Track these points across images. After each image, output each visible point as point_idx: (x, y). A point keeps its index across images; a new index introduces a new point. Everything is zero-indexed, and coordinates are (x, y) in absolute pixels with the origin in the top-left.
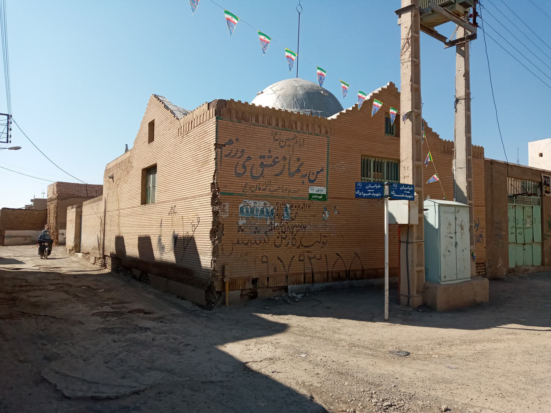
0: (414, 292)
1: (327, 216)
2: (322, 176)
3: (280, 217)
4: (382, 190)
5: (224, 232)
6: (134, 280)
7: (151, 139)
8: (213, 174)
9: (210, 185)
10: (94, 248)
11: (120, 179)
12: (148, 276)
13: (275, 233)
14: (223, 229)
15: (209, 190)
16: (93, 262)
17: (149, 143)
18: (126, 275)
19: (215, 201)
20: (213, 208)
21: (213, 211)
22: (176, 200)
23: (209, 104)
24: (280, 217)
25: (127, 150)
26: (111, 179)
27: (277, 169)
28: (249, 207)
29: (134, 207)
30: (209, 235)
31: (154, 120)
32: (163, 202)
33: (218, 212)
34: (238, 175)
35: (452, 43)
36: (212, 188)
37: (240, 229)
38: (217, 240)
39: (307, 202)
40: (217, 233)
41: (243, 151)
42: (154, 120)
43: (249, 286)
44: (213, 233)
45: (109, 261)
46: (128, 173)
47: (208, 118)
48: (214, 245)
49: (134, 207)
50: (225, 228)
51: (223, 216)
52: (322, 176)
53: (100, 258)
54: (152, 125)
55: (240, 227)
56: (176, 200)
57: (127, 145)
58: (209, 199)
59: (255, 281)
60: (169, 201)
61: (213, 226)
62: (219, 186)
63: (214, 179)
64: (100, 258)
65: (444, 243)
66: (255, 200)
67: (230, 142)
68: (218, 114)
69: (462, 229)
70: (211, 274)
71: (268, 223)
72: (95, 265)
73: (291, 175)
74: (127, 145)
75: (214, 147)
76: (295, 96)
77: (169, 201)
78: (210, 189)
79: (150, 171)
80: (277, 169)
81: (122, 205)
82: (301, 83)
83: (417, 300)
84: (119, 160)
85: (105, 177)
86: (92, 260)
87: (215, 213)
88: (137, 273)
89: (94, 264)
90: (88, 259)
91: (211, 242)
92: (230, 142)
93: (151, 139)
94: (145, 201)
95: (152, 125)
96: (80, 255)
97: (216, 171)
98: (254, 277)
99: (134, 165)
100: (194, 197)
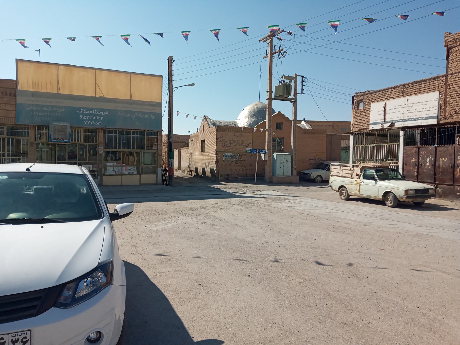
0: (267, 178)
2: (251, 145)
3: (236, 158)
4: (257, 151)
7: (204, 131)
10: (187, 168)
13: (234, 162)
19: (216, 154)
24: (236, 158)
27: (235, 144)
34: (223, 146)
35: (292, 102)
37: (223, 161)
39: (245, 153)
43: (226, 176)
44: (216, 162)
52: (251, 145)
54: (204, 125)
59: (228, 175)
65: (278, 165)
67: (221, 138)
68: (217, 130)
69: (287, 161)
73: (240, 145)
76: (254, 112)
79: (203, 141)
80: (235, 144)
82: (258, 106)
83: (268, 180)
86: (186, 172)
87: (216, 157)
90: (184, 172)
92: (221, 138)
93: (204, 131)
94: (202, 151)
95: (204, 125)
96: (181, 171)
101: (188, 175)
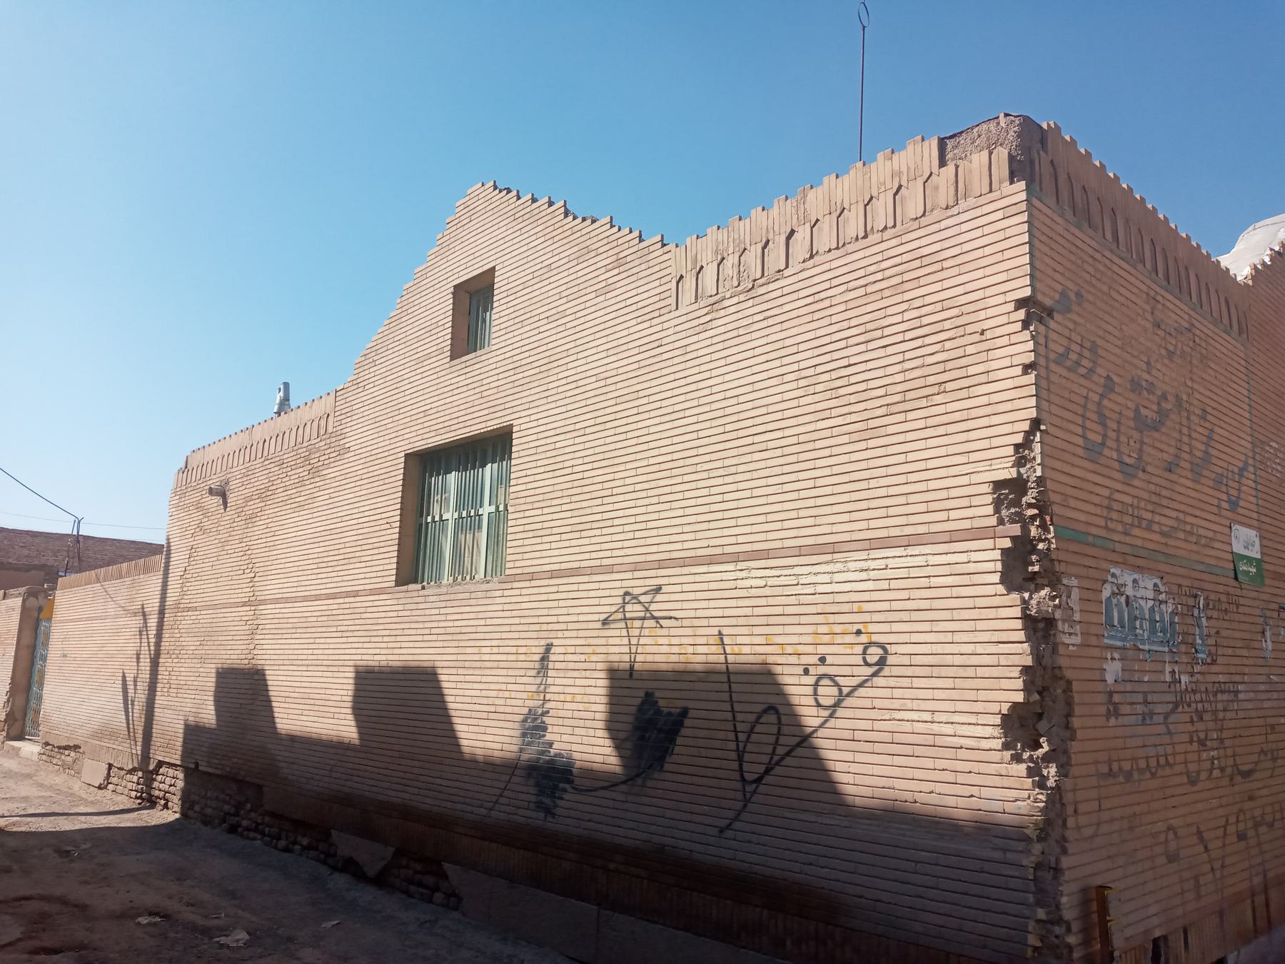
1: (1269, 643)
5: (1076, 722)
6: (340, 881)
8: (1019, 439)
9: (987, 488)
10: (105, 733)
11: (264, 495)
12: (444, 876)
14: (1069, 703)
15: (984, 511)
16: (99, 780)
17: (453, 358)
18: (286, 850)
19: (1019, 568)
20: (1025, 604)
21: (1026, 617)
22: (660, 564)
23: (942, 144)
25: (284, 405)
26: (217, 500)
28: (1123, 599)
29: (356, 594)
30: (997, 732)
31: (493, 269)
32: (553, 575)
33: (1050, 622)
36: (997, 505)
38: (1047, 759)
40: (1043, 726)
41: (1094, 349)
42: (493, 269)
45: (172, 783)
46: (314, 472)
47: (944, 193)
48: (1041, 785)
49: (356, 594)
50: (1077, 698)
51: (1070, 639)
53: (132, 771)
55: (1111, 694)
56: (660, 564)
57: (286, 385)
58: (987, 558)
60: (610, 569)
61: (1026, 689)
62: (1053, 497)
63: (1020, 462)
64: (132, 771)
66: (1139, 569)
70: (1033, 940)
71: (1168, 678)
72: (107, 793)
74: (286, 385)
75: (1021, 314)
77: (610, 569)
78: (990, 510)
81: (271, 588)
84: (258, 435)
85: (180, 491)
86: (94, 771)
87: (1039, 628)
88: (372, 855)
89: (100, 788)
91: (1021, 769)
94: (413, 565)
96: (29, 749)
97: (1036, 423)
98: (1157, 933)
99: (350, 441)
100: (832, 549)
101: (123, 794)
